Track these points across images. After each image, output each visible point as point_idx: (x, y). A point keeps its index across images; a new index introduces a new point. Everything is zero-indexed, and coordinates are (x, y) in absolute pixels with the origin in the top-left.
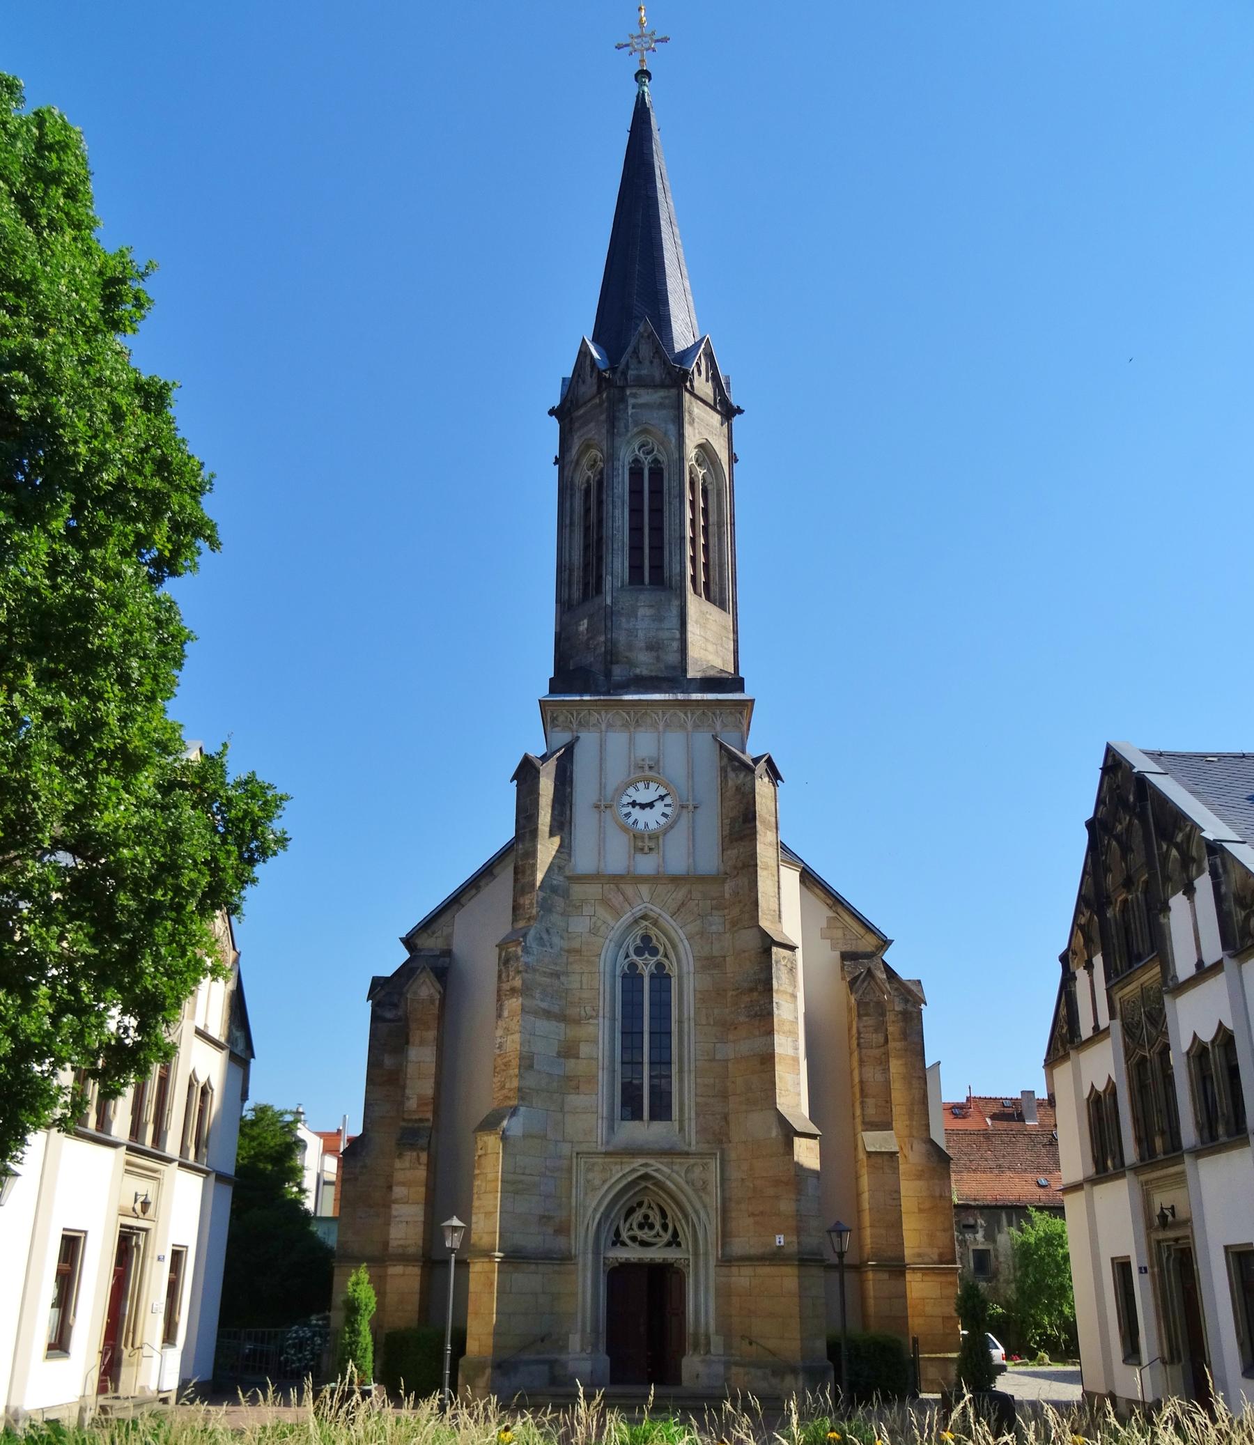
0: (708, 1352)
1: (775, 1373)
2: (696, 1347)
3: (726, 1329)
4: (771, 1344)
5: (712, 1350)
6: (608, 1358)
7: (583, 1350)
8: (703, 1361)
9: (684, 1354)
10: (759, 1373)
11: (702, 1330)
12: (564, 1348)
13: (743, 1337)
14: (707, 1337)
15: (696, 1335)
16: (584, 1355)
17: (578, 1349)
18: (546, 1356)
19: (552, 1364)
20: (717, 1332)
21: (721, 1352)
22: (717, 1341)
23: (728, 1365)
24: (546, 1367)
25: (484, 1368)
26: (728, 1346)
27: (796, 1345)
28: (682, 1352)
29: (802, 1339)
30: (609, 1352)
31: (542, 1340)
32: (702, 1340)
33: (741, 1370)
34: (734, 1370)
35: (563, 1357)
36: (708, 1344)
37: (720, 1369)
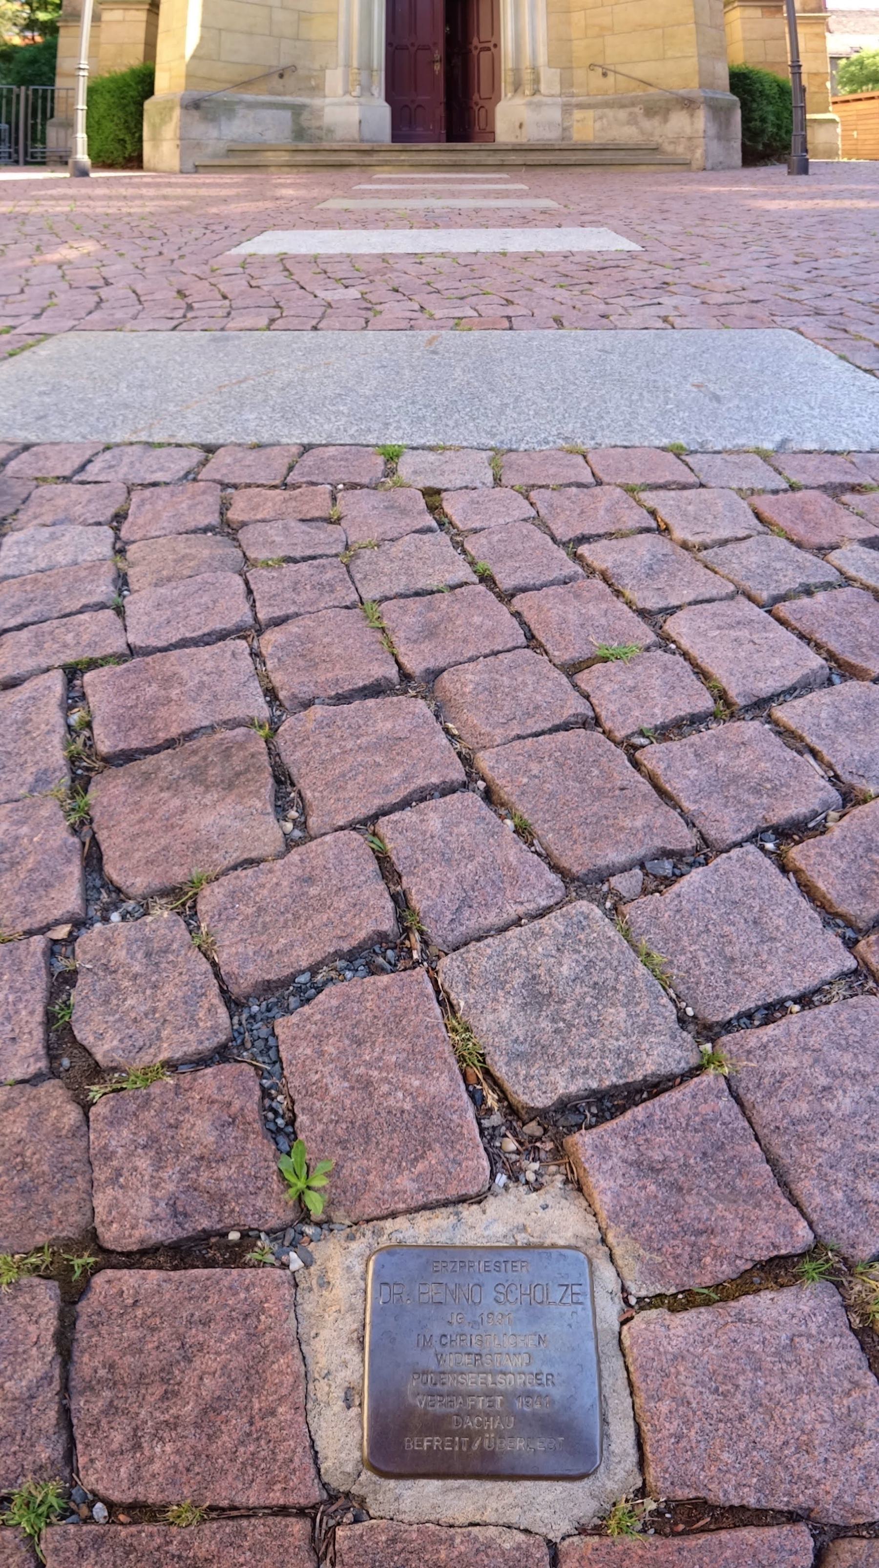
0: (536, 92)
1: (651, 111)
2: (517, 87)
3: (564, 61)
4: (641, 71)
5: (543, 87)
6: (386, 110)
7: (347, 92)
8: (529, 104)
9: (499, 99)
10: (622, 114)
11: (527, 62)
12: (317, 89)
13: (592, 67)
14: (535, 69)
15: (517, 71)
16: (348, 98)
17: (340, 91)
18: (287, 99)
19: (297, 110)
20: (550, 64)
21: (557, 90)
22: (550, 80)
23: (567, 109)
24: (287, 115)
25: (172, 109)
26: (566, 83)
27: (691, 65)
28: (495, 96)
29: (700, 56)
30: (388, 99)
31: (281, 76)
32: (527, 76)
33: (590, 114)
34: (578, 114)
35: (317, 102)
36: (537, 81)
37: (555, 114)
